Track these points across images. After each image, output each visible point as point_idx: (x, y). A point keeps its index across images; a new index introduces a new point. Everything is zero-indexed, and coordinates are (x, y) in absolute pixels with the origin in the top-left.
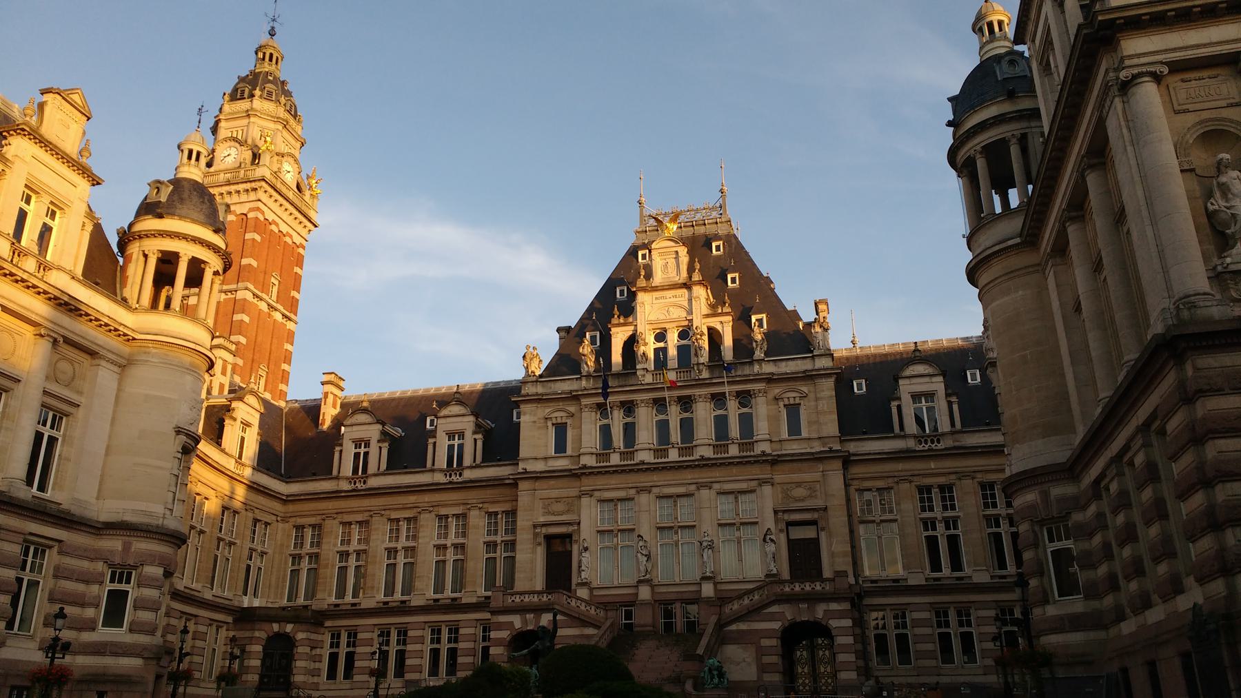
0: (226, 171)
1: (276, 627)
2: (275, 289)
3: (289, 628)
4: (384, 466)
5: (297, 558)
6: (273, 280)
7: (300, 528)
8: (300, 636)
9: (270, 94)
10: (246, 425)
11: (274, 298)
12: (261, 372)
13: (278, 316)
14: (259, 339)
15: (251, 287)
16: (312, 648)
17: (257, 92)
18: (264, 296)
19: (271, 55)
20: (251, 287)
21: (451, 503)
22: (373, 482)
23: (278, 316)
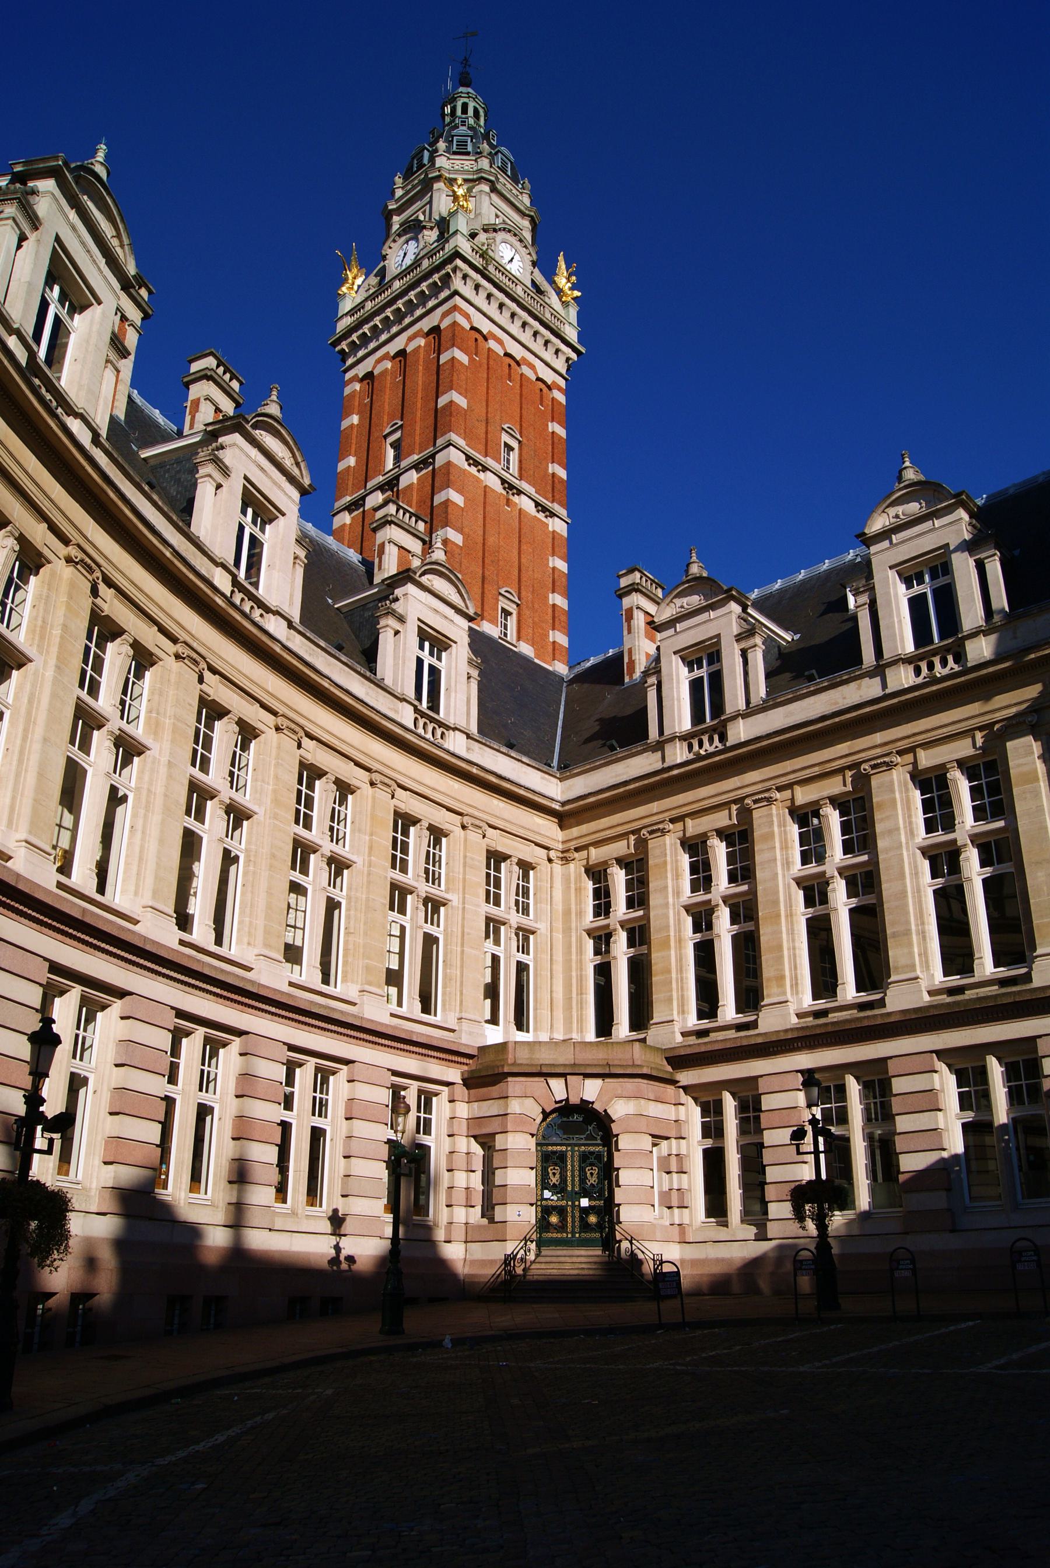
0: (400, 276)
1: (557, 1086)
2: (514, 457)
3: (591, 1090)
4: (760, 690)
5: (602, 940)
6: (505, 438)
7: (597, 874)
8: (619, 1110)
9: (462, 144)
10: (434, 641)
11: (514, 468)
12: (503, 603)
13: (526, 504)
14: (491, 540)
15: (461, 442)
16: (657, 1138)
17: (442, 145)
18: (490, 462)
19: (465, 107)
20: (461, 442)
21: (948, 741)
22: (741, 731)
23: (526, 504)
